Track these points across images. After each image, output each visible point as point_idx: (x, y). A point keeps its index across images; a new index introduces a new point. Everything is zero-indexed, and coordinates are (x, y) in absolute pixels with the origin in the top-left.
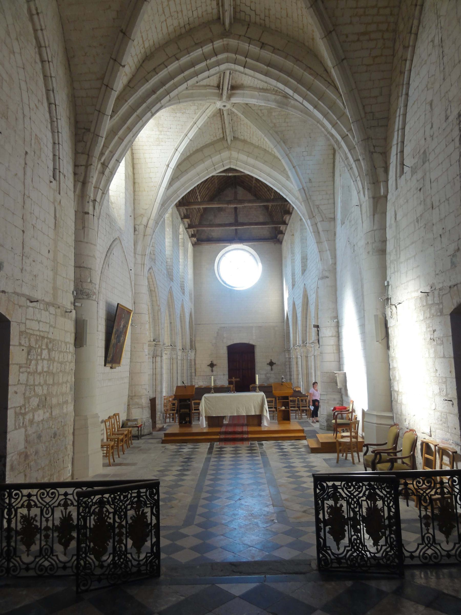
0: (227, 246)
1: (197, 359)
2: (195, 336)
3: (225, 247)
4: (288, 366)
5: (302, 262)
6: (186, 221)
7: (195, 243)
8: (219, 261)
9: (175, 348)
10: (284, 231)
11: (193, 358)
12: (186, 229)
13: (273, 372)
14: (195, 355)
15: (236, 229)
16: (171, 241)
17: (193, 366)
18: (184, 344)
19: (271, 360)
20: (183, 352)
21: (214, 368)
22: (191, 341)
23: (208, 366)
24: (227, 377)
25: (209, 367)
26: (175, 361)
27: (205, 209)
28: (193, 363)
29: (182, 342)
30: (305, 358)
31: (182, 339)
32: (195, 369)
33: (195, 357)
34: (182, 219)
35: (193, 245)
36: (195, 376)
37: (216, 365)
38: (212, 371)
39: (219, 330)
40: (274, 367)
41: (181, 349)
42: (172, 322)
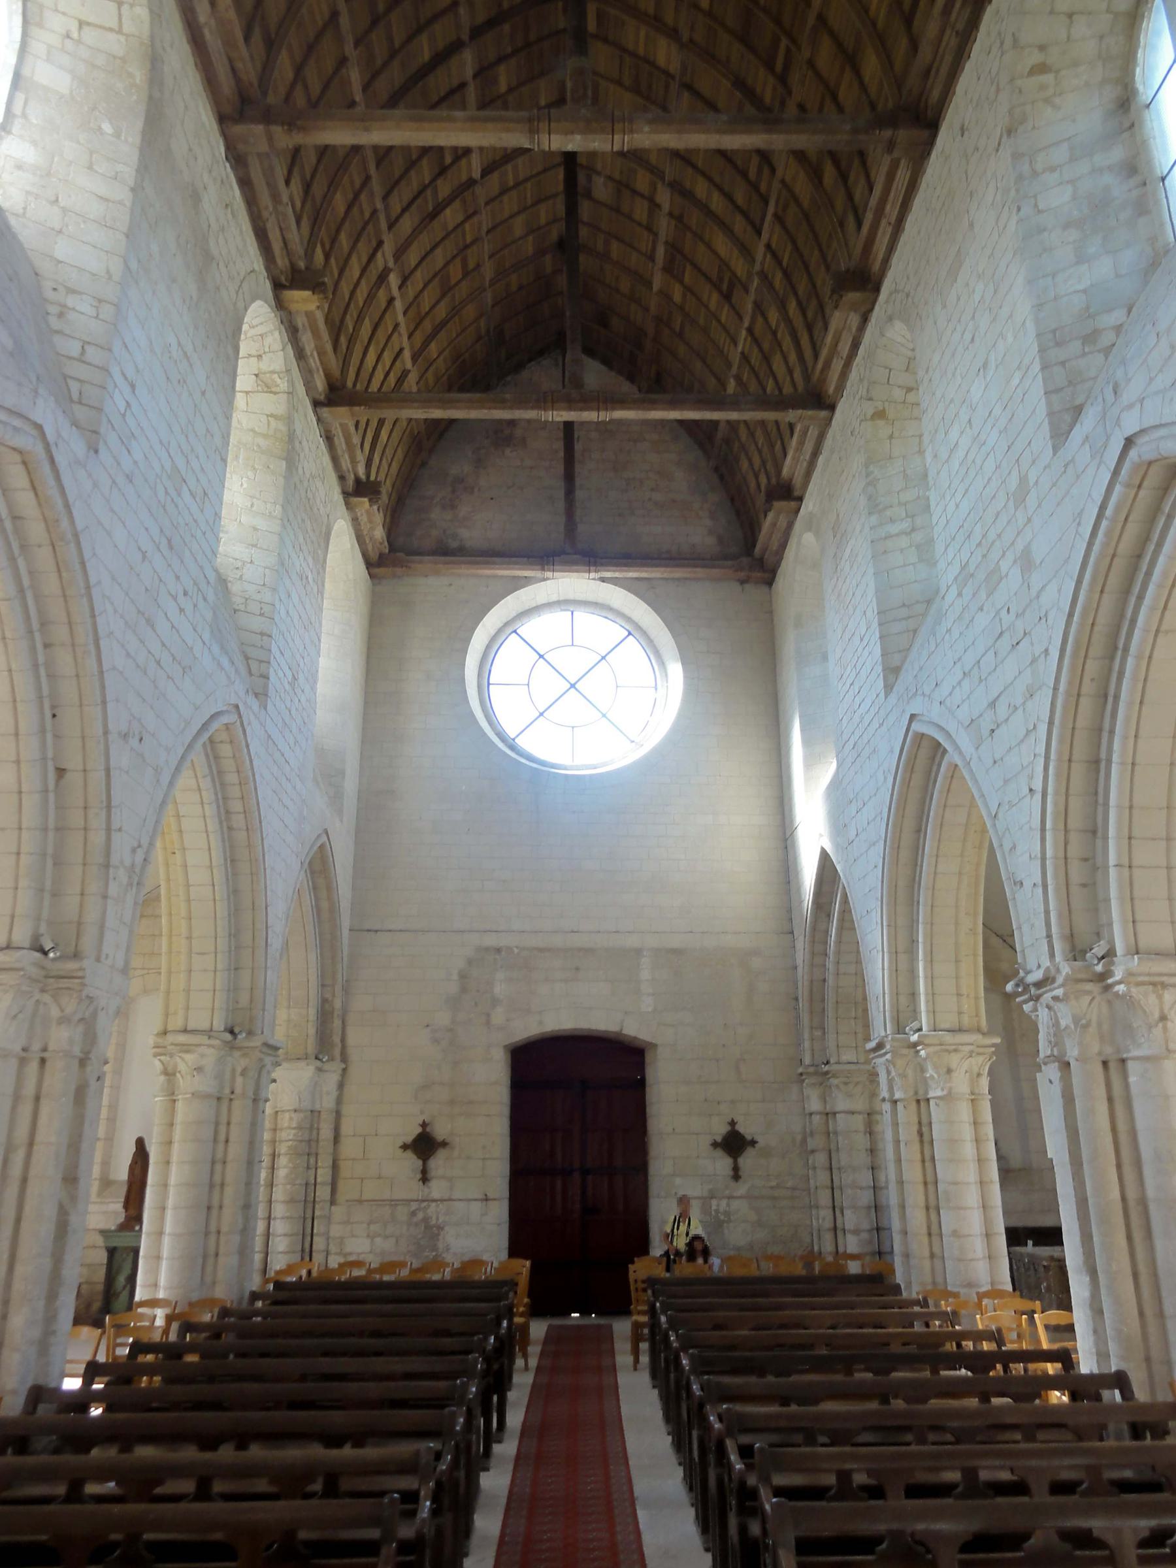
0: (527, 581)
1: (346, 1110)
2: (346, 990)
3: (518, 584)
4: (820, 1159)
5: (1045, 367)
6: (303, 301)
7: (381, 555)
8: (488, 647)
9: (71, 965)
10: (797, 481)
11: (328, 1103)
12: (316, 404)
13: (742, 1189)
14: (341, 1086)
15: (568, 426)
16: (122, 194)
17: (325, 1148)
18: (244, 999)
19: (733, 1123)
20: (231, 1047)
21: (438, 1163)
22: (325, 1015)
23: (405, 1147)
24: (500, 1211)
25: (410, 1154)
26: (59, 1079)
27: (439, 430)
28: (326, 1132)
29: (233, 989)
30: (1099, 1068)
31: (235, 969)
32: (335, 1167)
33: (339, 1101)
34: (278, 286)
35: (369, 564)
36: (333, 1202)
37: (444, 1144)
38: (425, 1178)
39: (470, 962)
40: (748, 1160)
41: (219, 1025)
42: (73, 762)
